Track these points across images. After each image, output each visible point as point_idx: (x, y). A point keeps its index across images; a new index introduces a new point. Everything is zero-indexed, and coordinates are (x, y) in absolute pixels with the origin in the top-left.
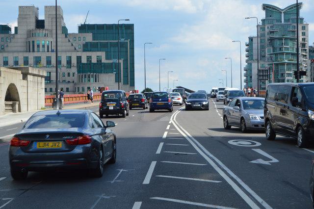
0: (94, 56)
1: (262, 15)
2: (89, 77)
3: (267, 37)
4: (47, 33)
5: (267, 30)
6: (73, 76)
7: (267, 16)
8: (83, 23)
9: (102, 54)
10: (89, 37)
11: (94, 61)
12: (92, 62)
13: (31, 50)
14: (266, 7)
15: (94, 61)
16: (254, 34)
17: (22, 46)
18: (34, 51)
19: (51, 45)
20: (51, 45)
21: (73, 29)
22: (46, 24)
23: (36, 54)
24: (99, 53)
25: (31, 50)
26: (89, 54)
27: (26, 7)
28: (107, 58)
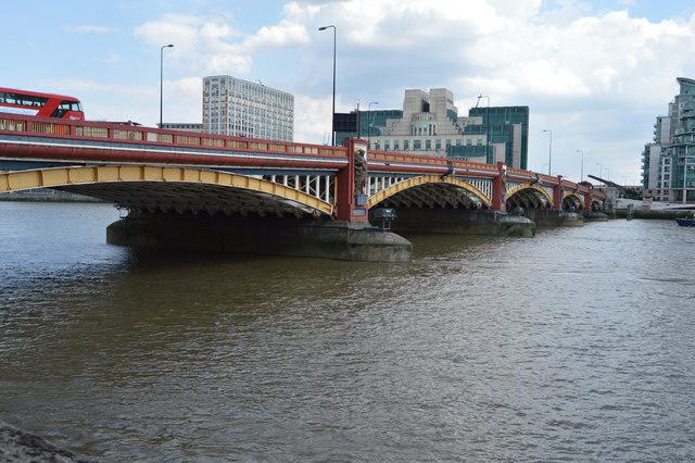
1: (677, 90)
3: (680, 116)
5: (680, 109)
7: (682, 90)
10: (479, 121)
14: (682, 81)
16: (665, 112)
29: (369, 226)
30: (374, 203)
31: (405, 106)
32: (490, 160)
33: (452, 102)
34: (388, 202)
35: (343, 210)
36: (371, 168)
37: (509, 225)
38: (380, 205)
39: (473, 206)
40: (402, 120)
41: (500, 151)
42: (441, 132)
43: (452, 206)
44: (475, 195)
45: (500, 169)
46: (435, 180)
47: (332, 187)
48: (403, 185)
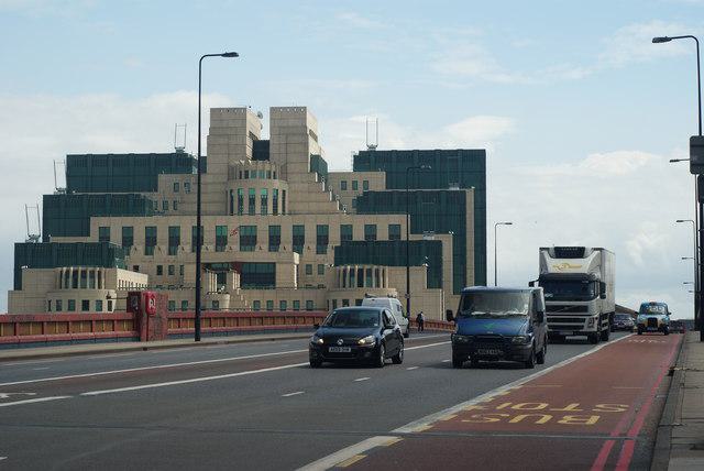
0: (383, 224)
2: (92, 276)
4: (273, 170)
6: (171, 273)
8: (365, 149)
10: (378, 181)
11: (383, 235)
13: (236, 211)
15: (383, 235)
17: (219, 202)
18: (240, 212)
19: (284, 198)
20: (284, 198)
21: (339, 161)
22: (272, 150)
26: (370, 219)
27: (228, 110)
28: (414, 230)
42: (300, 207)
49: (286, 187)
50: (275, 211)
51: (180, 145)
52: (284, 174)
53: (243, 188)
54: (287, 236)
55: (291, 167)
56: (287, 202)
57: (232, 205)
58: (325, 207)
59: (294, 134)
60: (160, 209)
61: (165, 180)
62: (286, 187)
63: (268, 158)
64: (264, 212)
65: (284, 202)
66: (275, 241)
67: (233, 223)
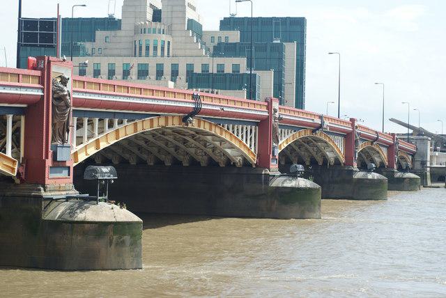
0: (228, 64)
8: (228, 16)
9: (242, 62)
10: (234, 36)
12: (210, 71)
13: (137, 54)
17: (128, 48)
18: (140, 55)
21: (211, 24)
23: (143, 60)
24: (236, 60)
25: (137, 54)
29: (75, 193)
30: (82, 158)
31: (124, 12)
32: (251, 95)
33: (194, 9)
34: (103, 157)
35: (33, 172)
36: (78, 103)
37: (402, 180)
38: (90, 161)
39: (229, 162)
40: (119, 33)
41: (266, 80)
42: (179, 52)
43: (180, 163)
44: (232, 147)
45: (269, 107)
46: (174, 123)
47: (16, 132)
48: (127, 131)
49: (170, 39)
50: (163, 55)
51: (111, 13)
52: (170, 31)
53: (143, 39)
54: (167, 70)
55: (174, 27)
56: (171, 49)
57: (137, 50)
58: (195, 52)
59: (177, 6)
60: (90, 52)
61: (100, 34)
62: (170, 39)
63: (160, 21)
64: (155, 55)
65: (168, 49)
66: (160, 74)
67: (135, 62)
